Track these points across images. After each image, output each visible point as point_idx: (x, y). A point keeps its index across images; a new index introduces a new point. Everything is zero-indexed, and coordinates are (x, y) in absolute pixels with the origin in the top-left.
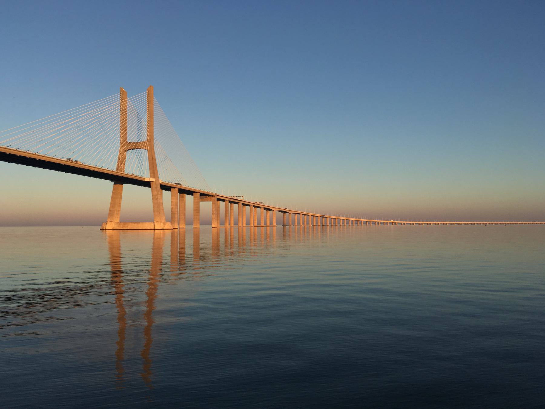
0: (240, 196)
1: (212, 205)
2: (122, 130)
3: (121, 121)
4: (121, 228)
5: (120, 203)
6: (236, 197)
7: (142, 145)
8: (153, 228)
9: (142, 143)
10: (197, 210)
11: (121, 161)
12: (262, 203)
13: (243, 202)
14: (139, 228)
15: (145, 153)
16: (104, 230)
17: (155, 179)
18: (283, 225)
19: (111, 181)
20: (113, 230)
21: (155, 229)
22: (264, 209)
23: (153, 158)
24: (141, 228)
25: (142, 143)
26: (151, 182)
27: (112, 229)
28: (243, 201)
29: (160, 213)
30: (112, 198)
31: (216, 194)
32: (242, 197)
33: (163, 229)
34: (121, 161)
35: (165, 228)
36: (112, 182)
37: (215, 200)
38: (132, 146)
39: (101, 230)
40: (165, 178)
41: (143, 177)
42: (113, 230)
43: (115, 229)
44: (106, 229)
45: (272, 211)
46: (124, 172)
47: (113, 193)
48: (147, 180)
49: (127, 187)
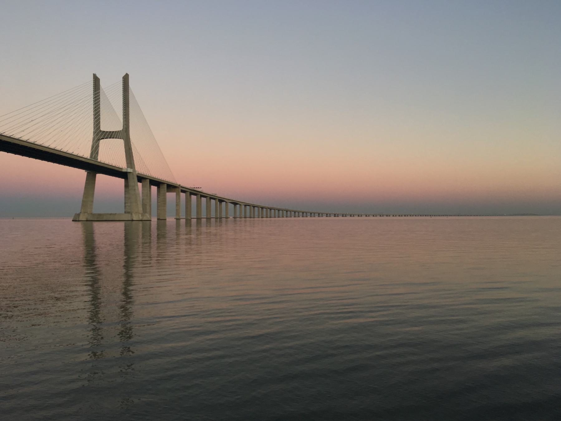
0: (198, 188)
1: (176, 197)
2: (95, 118)
3: (95, 109)
4: (96, 220)
5: (93, 194)
6: (194, 188)
7: (117, 135)
8: (129, 219)
9: (118, 133)
10: (162, 202)
11: (95, 149)
12: (216, 195)
13: (202, 194)
15: (119, 143)
17: (132, 170)
18: (233, 217)
19: (84, 171)
20: (87, 221)
21: (133, 220)
22: (219, 201)
23: (129, 148)
24: (117, 220)
25: (118, 133)
26: (128, 173)
27: (85, 220)
28: (202, 192)
29: (138, 204)
30: (85, 188)
31: (179, 185)
32: (201, 188)
33: (141, 221)
34: (95, 149)
35: (143, 219)
36: (86, 172)
37: (179, 191)
38: (108, 135)
39: (73, 221)
40: (140, 168)
41: (121, 168)
42: (87, 221)
43: (89, 220)
45: (225, 202)
46: (97, 159)
47: (86, 183)
48: (123, 171)
49: (100, 178)
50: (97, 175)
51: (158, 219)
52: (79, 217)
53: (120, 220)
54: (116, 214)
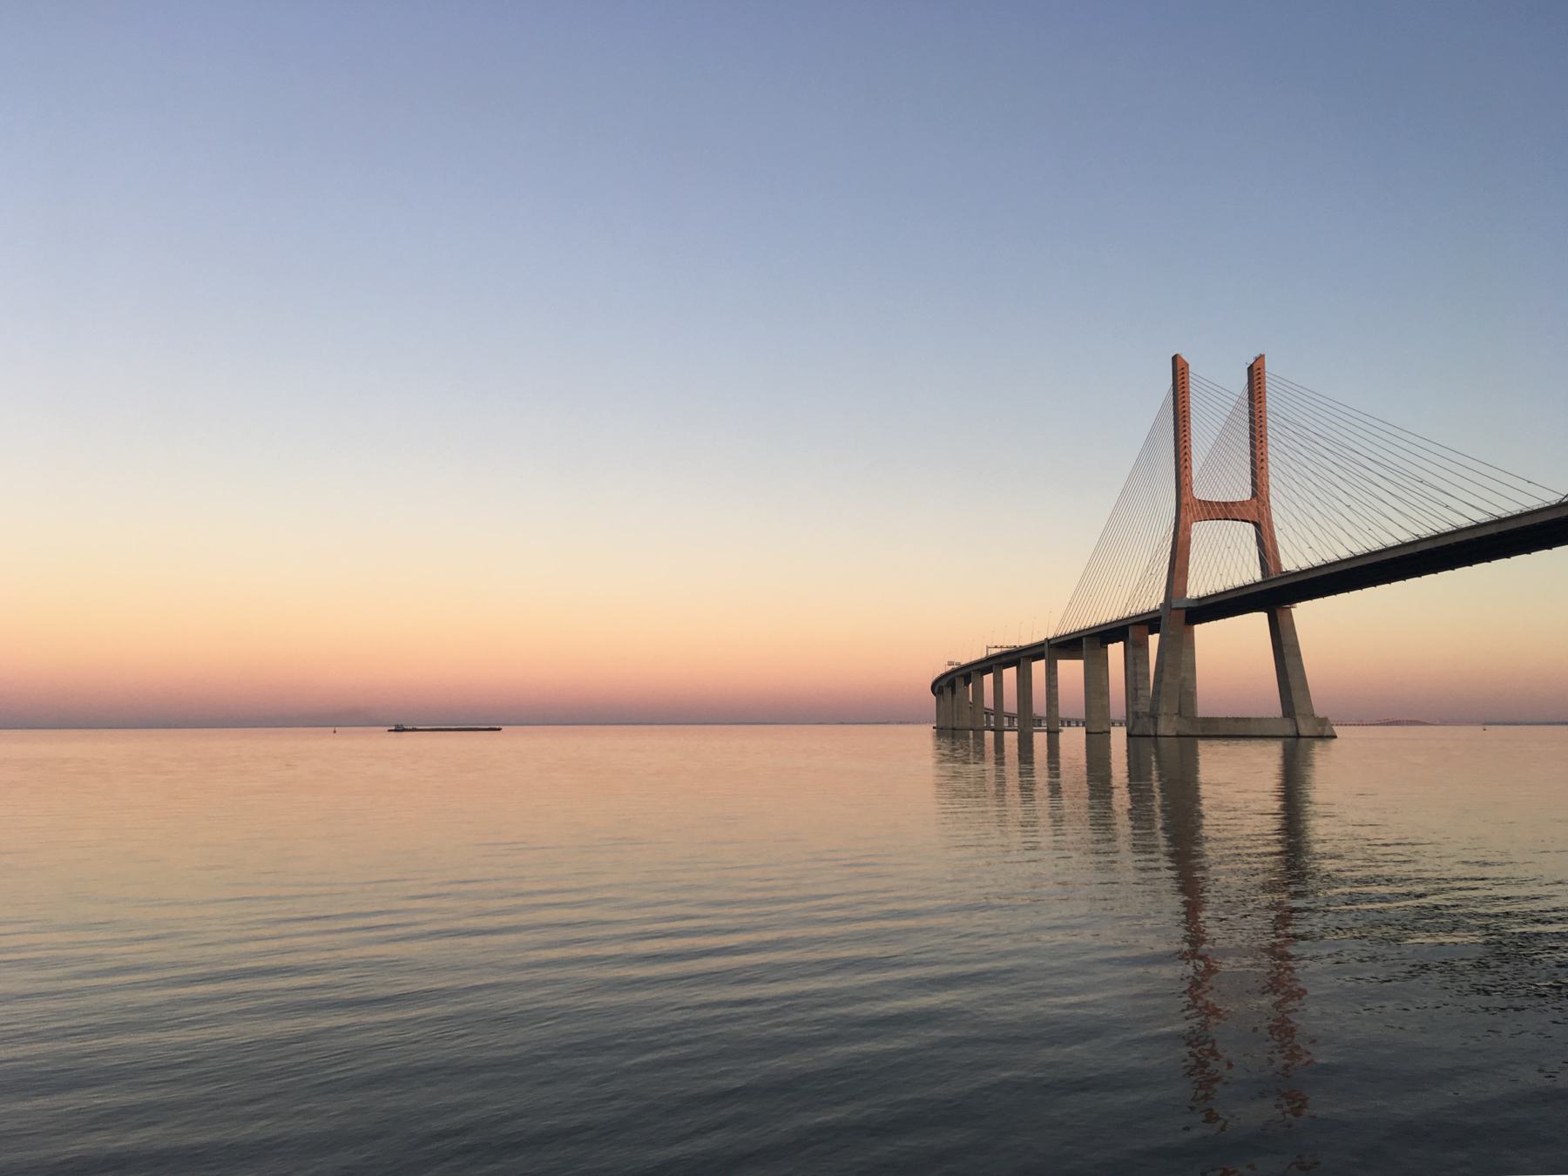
4: (1201, 733)
14: (1253, 733)
16: (1149, 736)
18: (935, 725)
20: (1177, 736)
21: (1298, 736)
24: (1258, 733)
27: (1174, 734)
35: (1327, 733)
42: (1177, 736)
43: (1182, 734)
44: (1159, 734)
50: (1266, 614)
51: (1087, 733)
52: (1156, 724)
53: (1265, 734)
54: (1249, 719)
